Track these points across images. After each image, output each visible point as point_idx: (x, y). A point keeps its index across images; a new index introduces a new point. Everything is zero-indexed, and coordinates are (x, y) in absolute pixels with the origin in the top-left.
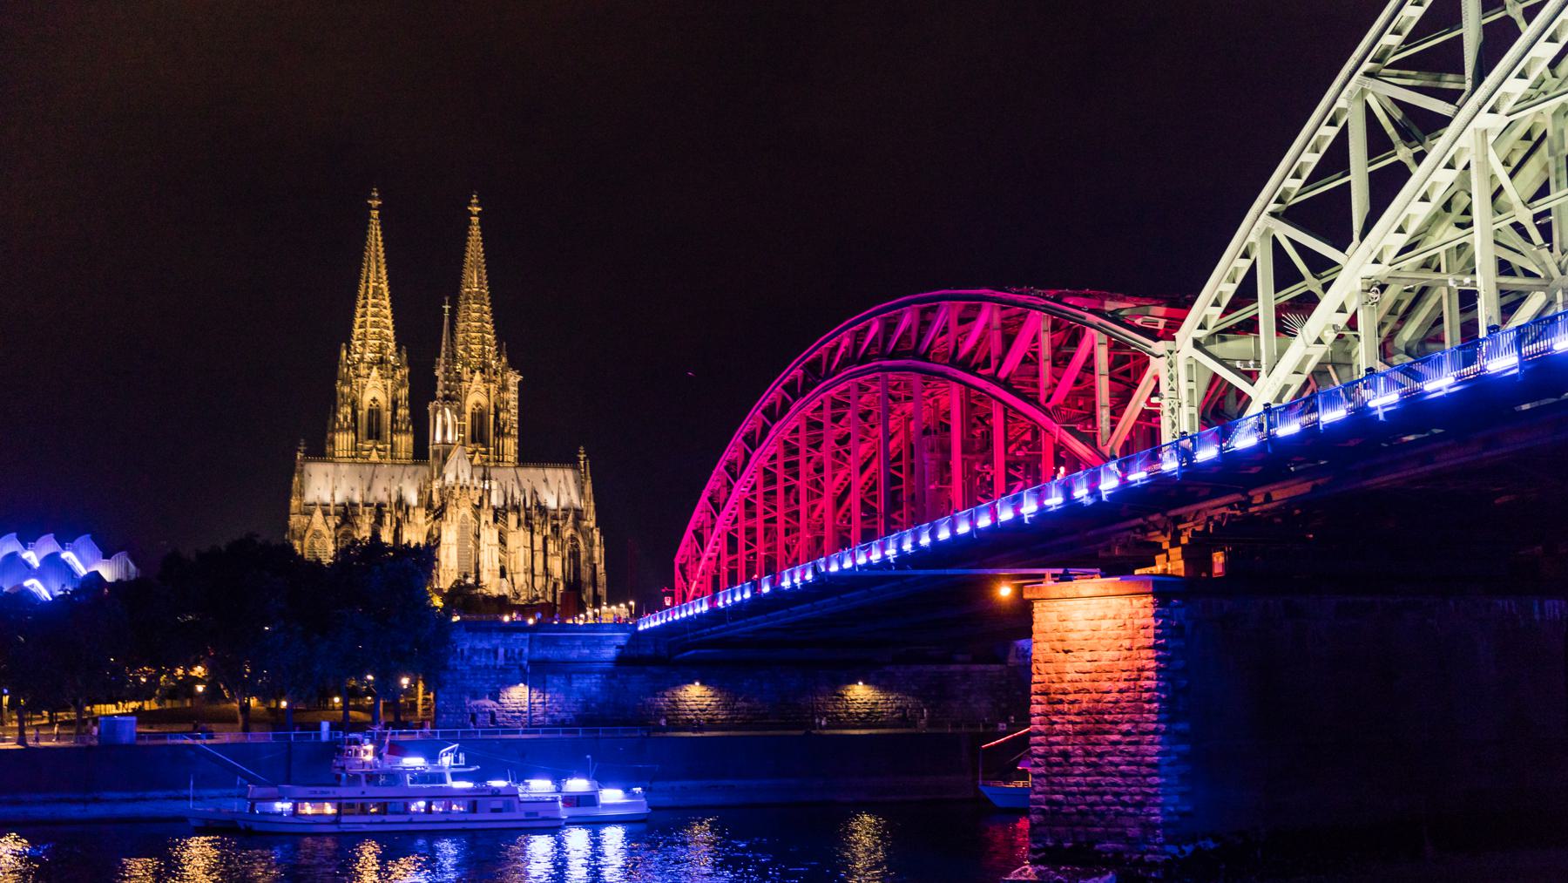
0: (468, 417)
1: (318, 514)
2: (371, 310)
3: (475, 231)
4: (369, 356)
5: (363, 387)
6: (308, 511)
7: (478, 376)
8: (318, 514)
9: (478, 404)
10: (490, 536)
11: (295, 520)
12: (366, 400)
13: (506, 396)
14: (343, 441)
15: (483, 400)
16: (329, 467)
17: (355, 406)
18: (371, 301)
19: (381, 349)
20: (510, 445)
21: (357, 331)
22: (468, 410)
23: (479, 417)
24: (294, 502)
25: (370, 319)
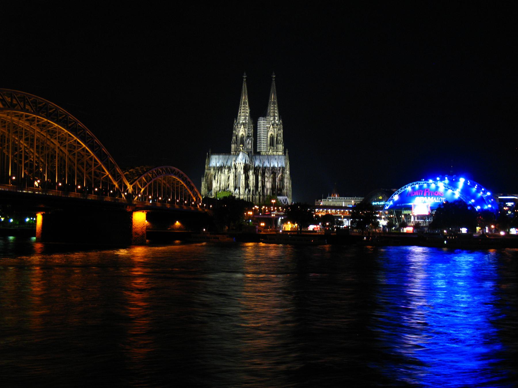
0: (269, 139)
1: (212, 170)
2: (242, 108)
3: (274, 83)
4: (241, 122)
5: (239, 131)
6: (209, 169)
7: (271, 127)
8: (212, 170)
9: (271, 134)
10: (243, 177)
11: (206, 171)
12: (240, 134)
13: (280, 132)
14: (233, 146)
15: (273, 134)
16: (217, 156)
17: (237, 136)
18: (243, 105)
19: (245, 119)
20: (281, 147)
21: (239, 114)
22: (269, 136)
23: (272, 138)
24: (206, 167)
25: (242, 111)
